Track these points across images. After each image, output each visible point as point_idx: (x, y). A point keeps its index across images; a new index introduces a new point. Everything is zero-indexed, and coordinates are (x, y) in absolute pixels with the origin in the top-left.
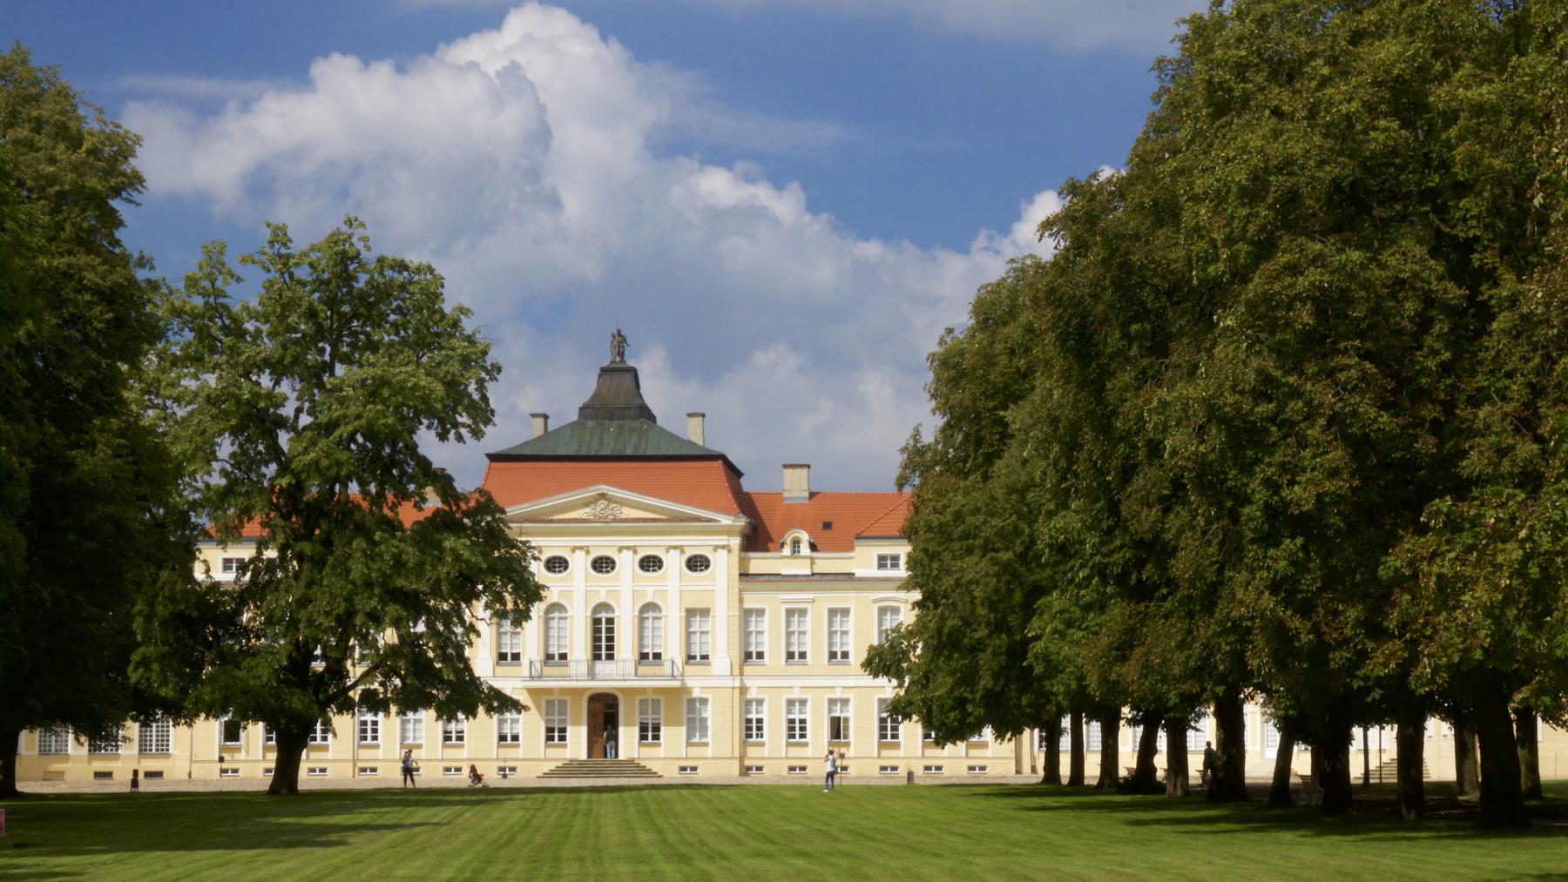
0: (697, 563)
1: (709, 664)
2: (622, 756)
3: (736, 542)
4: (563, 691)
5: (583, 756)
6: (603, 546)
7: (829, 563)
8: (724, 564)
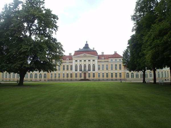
0: (94, 61)
3: (97, 58)
5: (83, 78)
6: (85, 59)
7: (106, 60)
8: (96, 61)
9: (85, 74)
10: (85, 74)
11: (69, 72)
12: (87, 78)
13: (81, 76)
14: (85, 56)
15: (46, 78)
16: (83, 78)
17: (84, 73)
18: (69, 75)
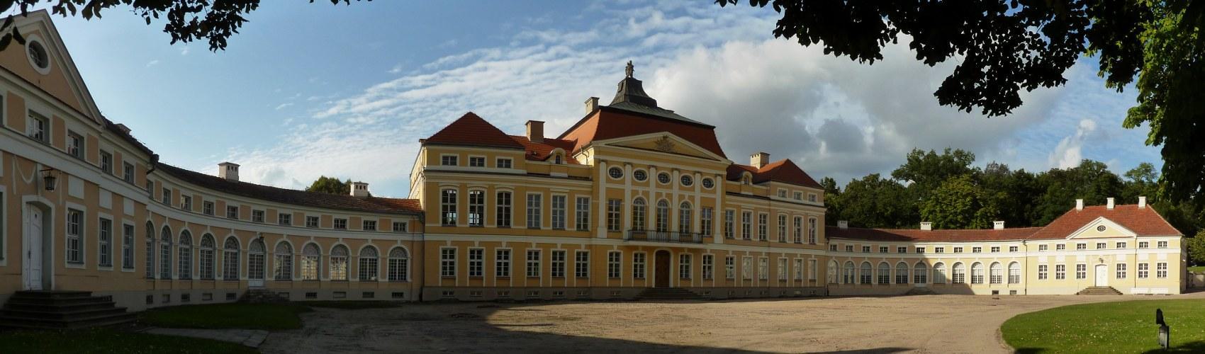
1: (712, 237)
2: (672, 285)
3: (725, 173)
4: (645, 248)
5: (654, 286)
7: (760, 189)
8: (718, 183)
9: (663, 257)
10: (663, 257)
11: (572, 242)
12: (674, 281)
13: (639, 274)
14: (664, 147)
15: (403, 277)
16: (650, 280)
17: (657, 254)
18: (570, 265)
